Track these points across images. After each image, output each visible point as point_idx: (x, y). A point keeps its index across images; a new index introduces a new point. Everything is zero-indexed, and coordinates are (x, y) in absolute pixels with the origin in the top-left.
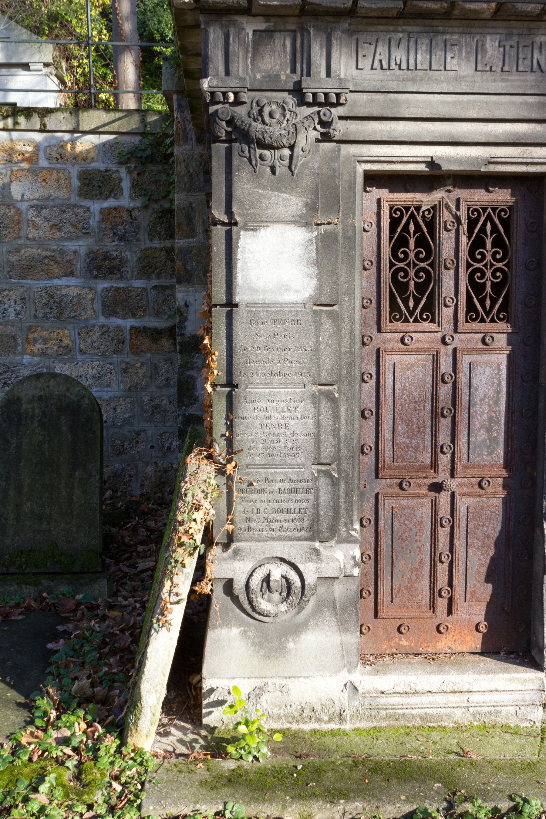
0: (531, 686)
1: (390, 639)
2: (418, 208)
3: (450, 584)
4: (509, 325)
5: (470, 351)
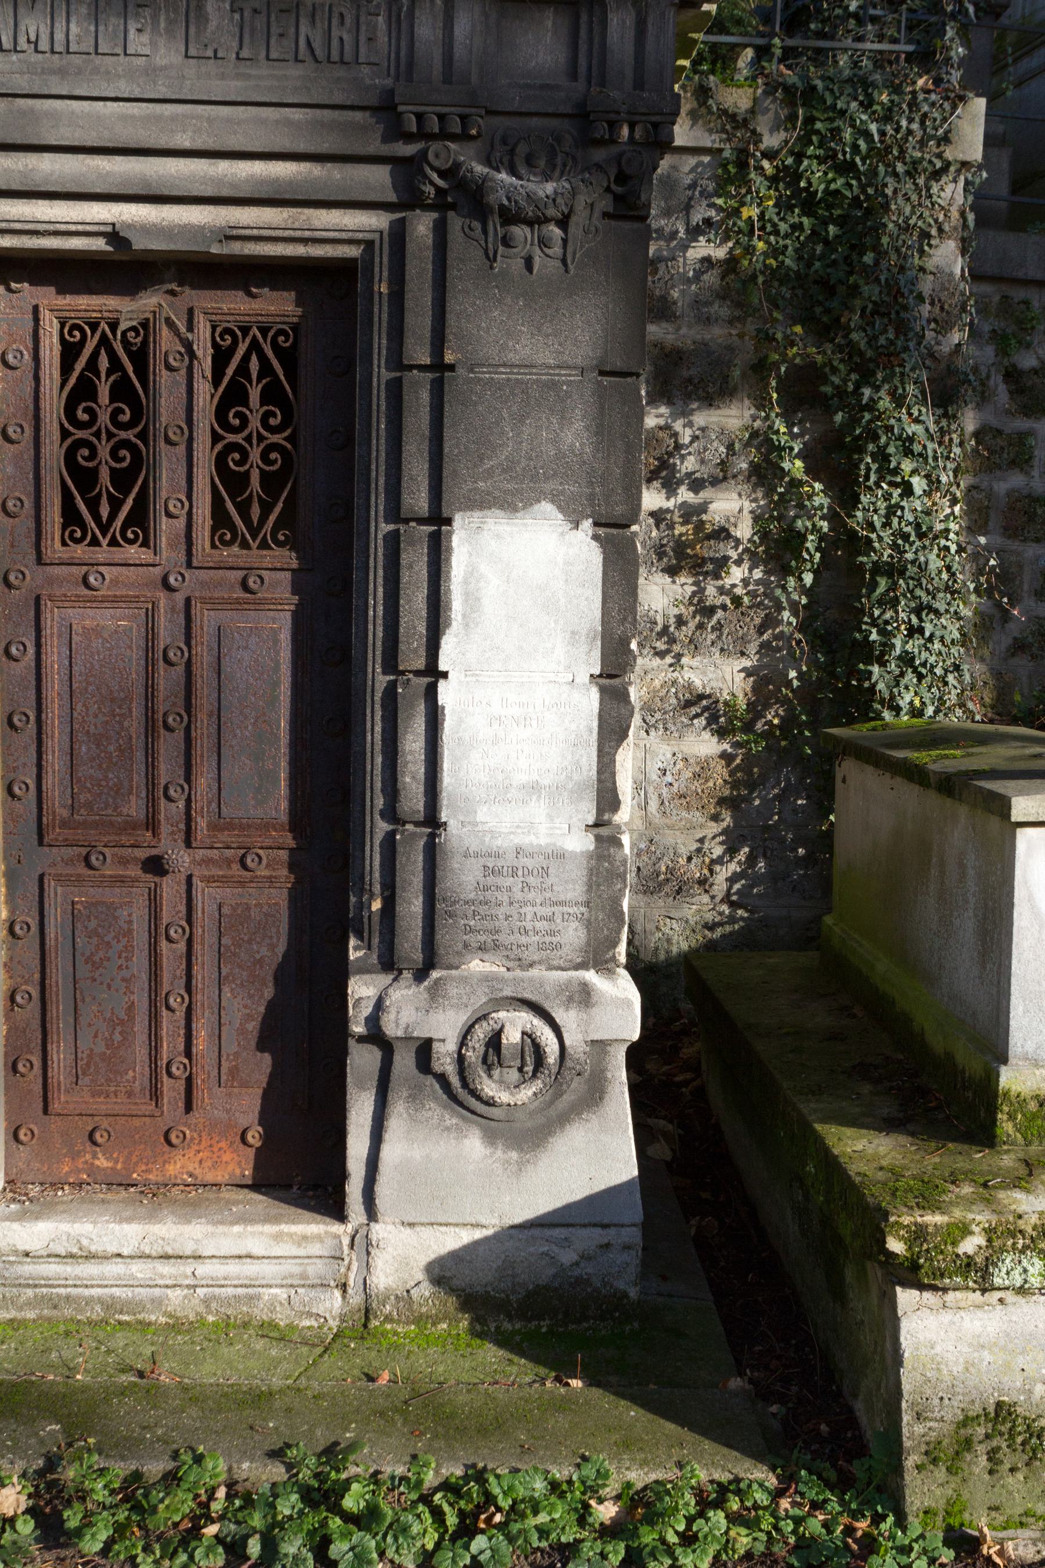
0: (316, 1249)
1: (75, 1156)
2: (114, 325)
3: (188, 1054)
4: (294, 554)
5: (214, 604)
